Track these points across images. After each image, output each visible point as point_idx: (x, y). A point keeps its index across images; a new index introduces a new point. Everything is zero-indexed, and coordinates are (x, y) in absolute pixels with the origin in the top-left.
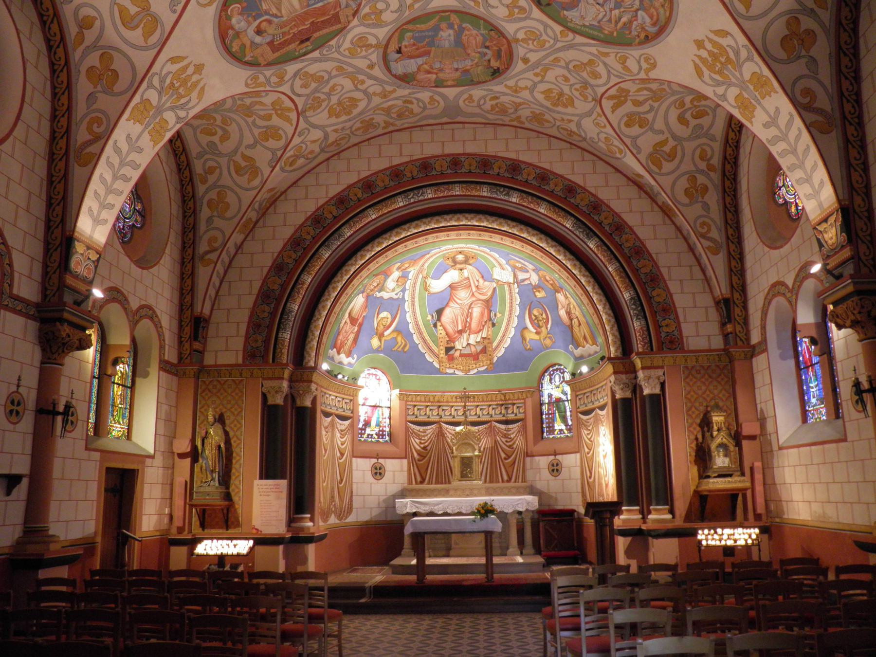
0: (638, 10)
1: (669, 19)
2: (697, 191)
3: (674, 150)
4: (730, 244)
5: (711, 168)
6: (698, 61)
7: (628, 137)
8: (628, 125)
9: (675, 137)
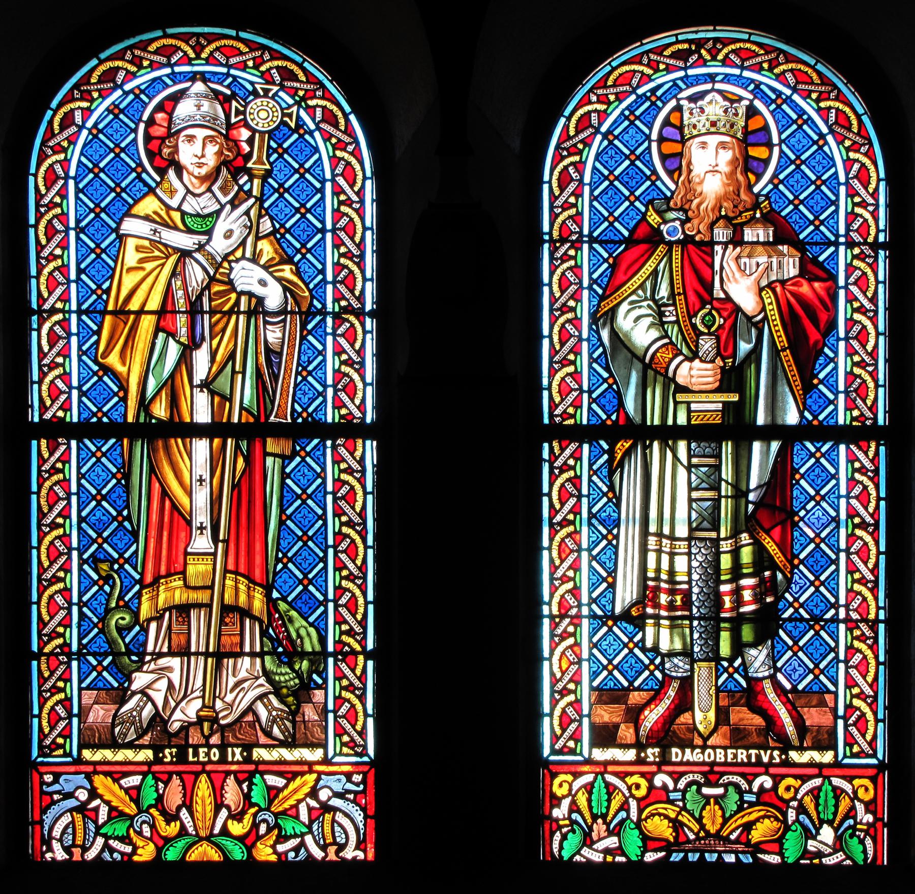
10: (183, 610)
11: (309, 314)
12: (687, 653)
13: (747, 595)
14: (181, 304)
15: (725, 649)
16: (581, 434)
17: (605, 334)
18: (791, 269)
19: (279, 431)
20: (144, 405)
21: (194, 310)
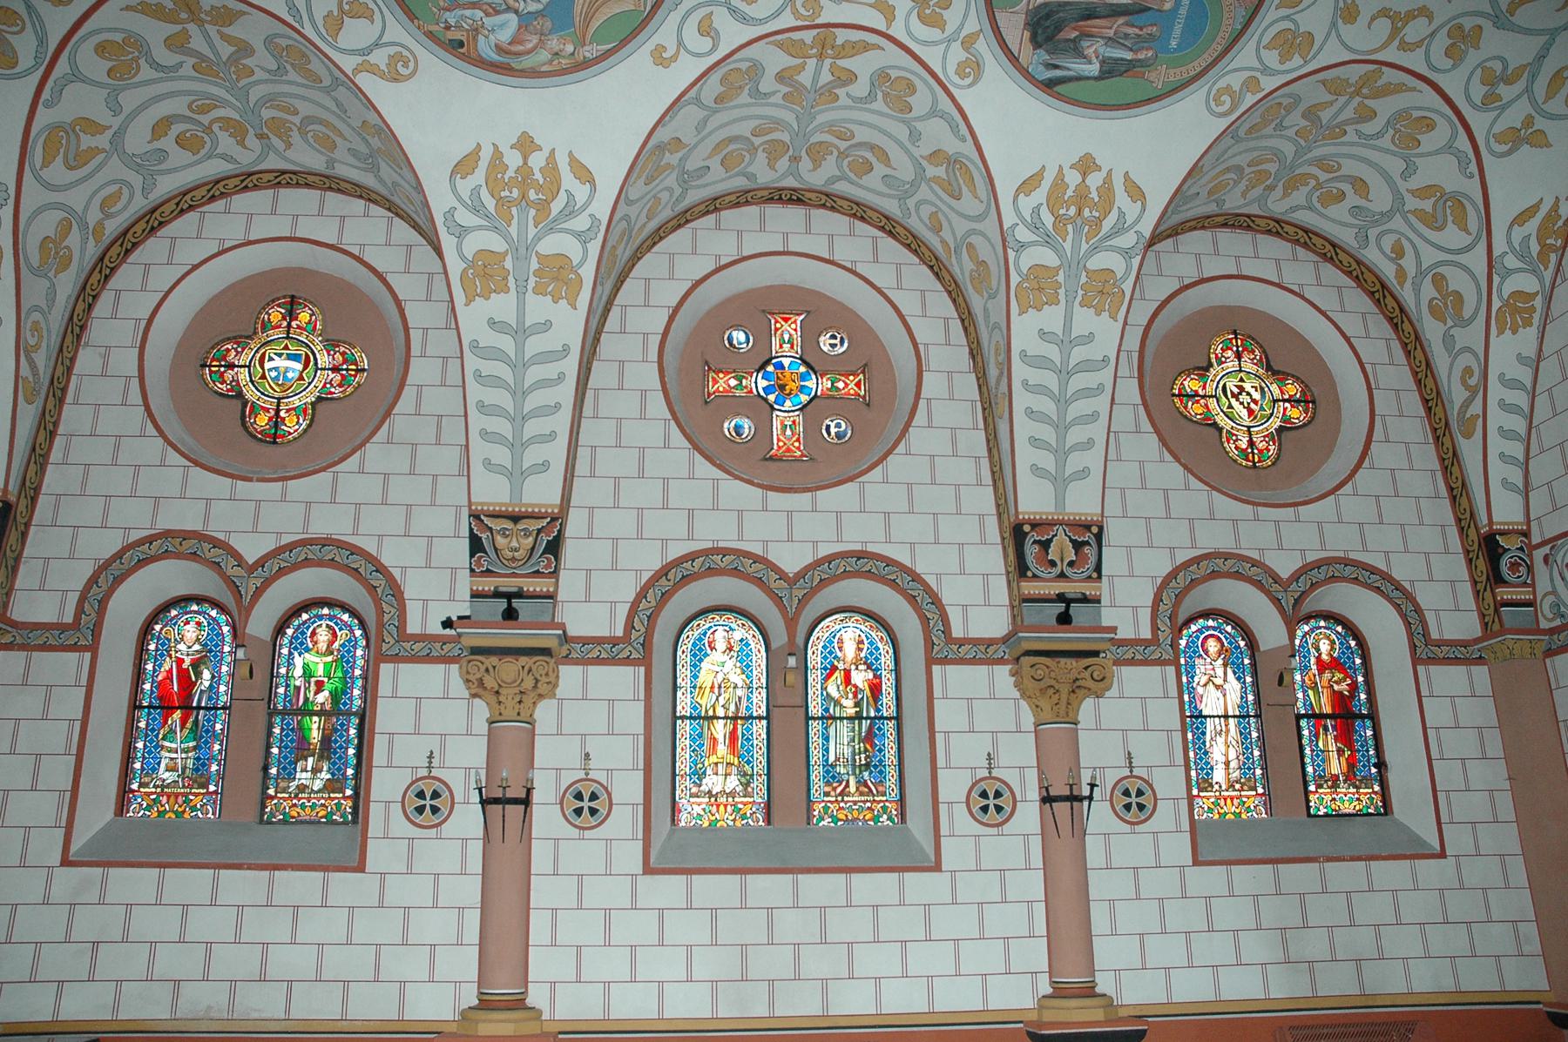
0: (516, 12)
1: (534, 73)
2: (57, 253)
3: (96, 151)
4: (51, 397)
5: (99, 229)
6: (486, 154)
7: (72, 61)
8: (101, 49)
9: (119, 135)
10: (716, 764)
11: (749, 688)
12: (848, 773)
13: (863, 759)
14: (716, 686)
15: (857, 772)
16: (818, 718)
17: (825, 693)
18: (871, 675)
19: (741, 718)
20: (706, 711)
21: (720, 687)
